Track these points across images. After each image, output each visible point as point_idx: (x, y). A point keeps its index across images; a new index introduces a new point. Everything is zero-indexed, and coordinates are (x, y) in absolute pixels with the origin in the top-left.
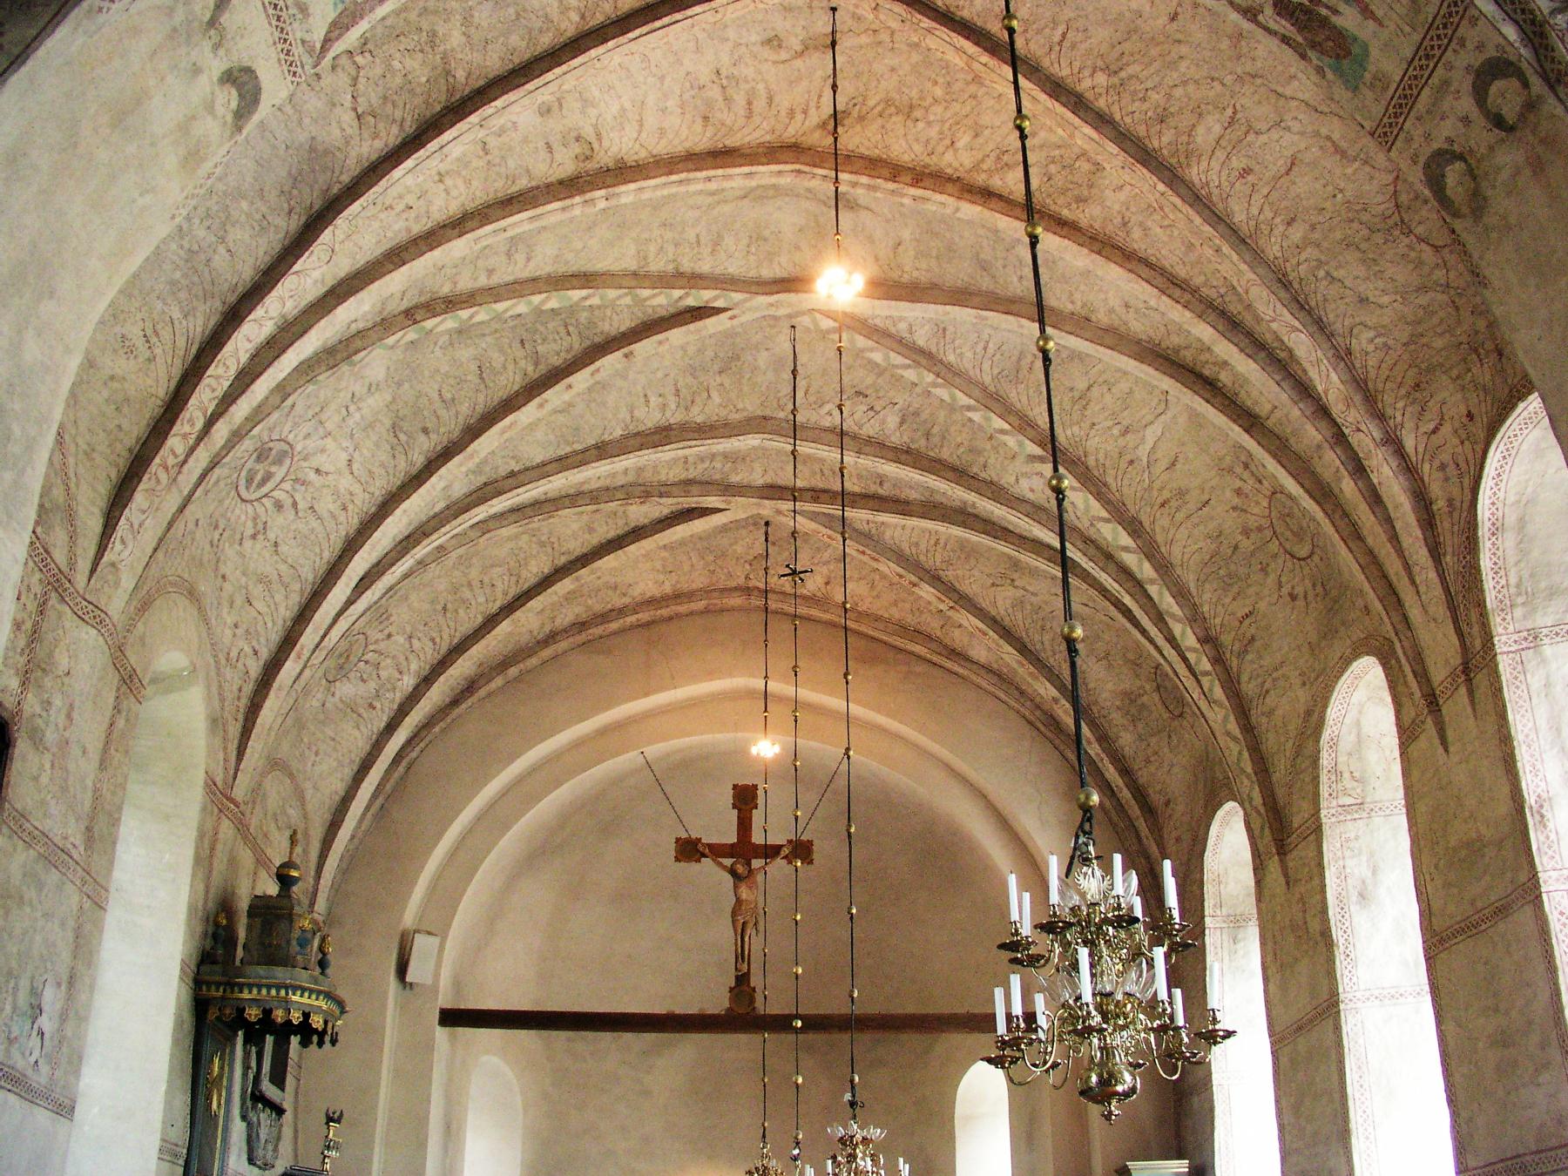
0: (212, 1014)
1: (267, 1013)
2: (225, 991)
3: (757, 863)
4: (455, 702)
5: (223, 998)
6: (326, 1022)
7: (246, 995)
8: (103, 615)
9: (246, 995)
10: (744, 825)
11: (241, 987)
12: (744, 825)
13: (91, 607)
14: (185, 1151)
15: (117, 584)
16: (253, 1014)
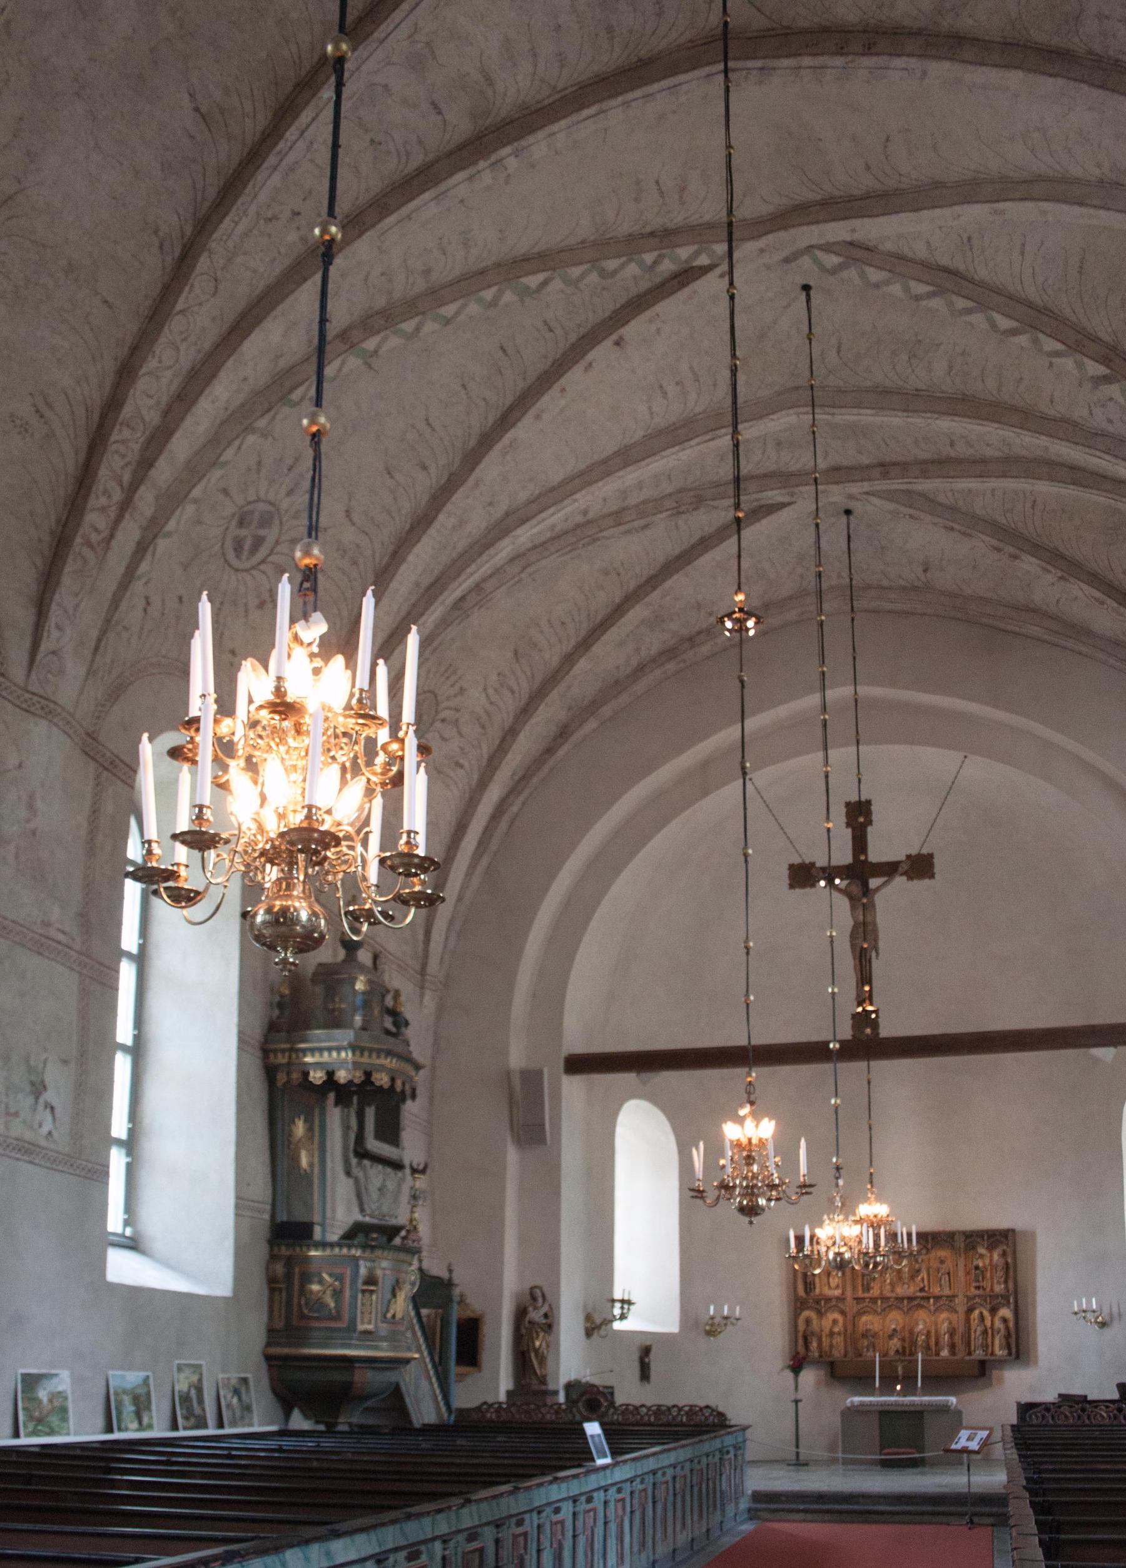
0: (281, 1078)
1: (330, 1074)
2: (290, 1057)
3: (874, 883)
4: (550, 751)
5: (289, 1064)
6: (393, 1080)
7: (308, 1059)
8: (52, 705)
9: (308, 1059)
10: (860, 843)
11: (304, 1051)
12: (860, 843)
13: (35, 698)
14: (268, 1207)
15: (61, 672)
16: (317, 1077)
